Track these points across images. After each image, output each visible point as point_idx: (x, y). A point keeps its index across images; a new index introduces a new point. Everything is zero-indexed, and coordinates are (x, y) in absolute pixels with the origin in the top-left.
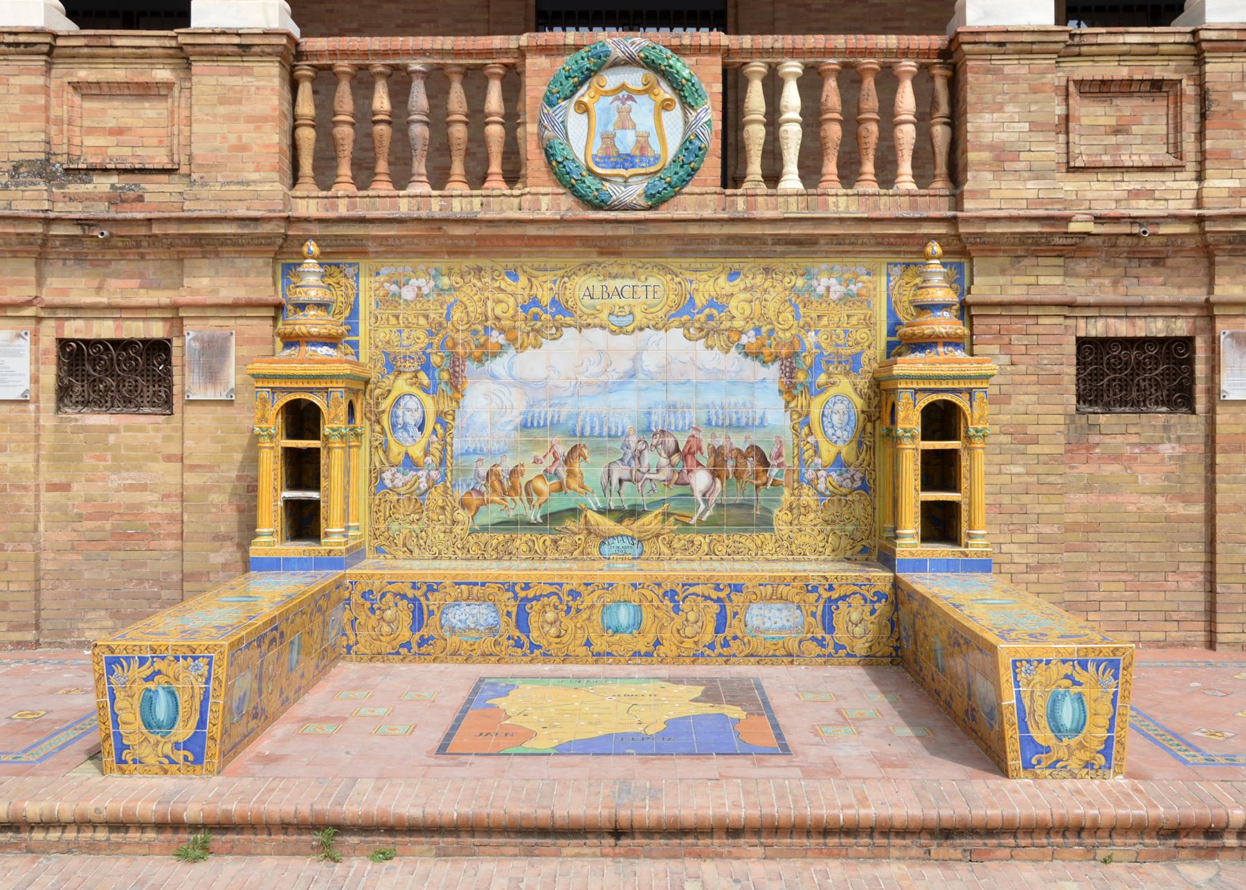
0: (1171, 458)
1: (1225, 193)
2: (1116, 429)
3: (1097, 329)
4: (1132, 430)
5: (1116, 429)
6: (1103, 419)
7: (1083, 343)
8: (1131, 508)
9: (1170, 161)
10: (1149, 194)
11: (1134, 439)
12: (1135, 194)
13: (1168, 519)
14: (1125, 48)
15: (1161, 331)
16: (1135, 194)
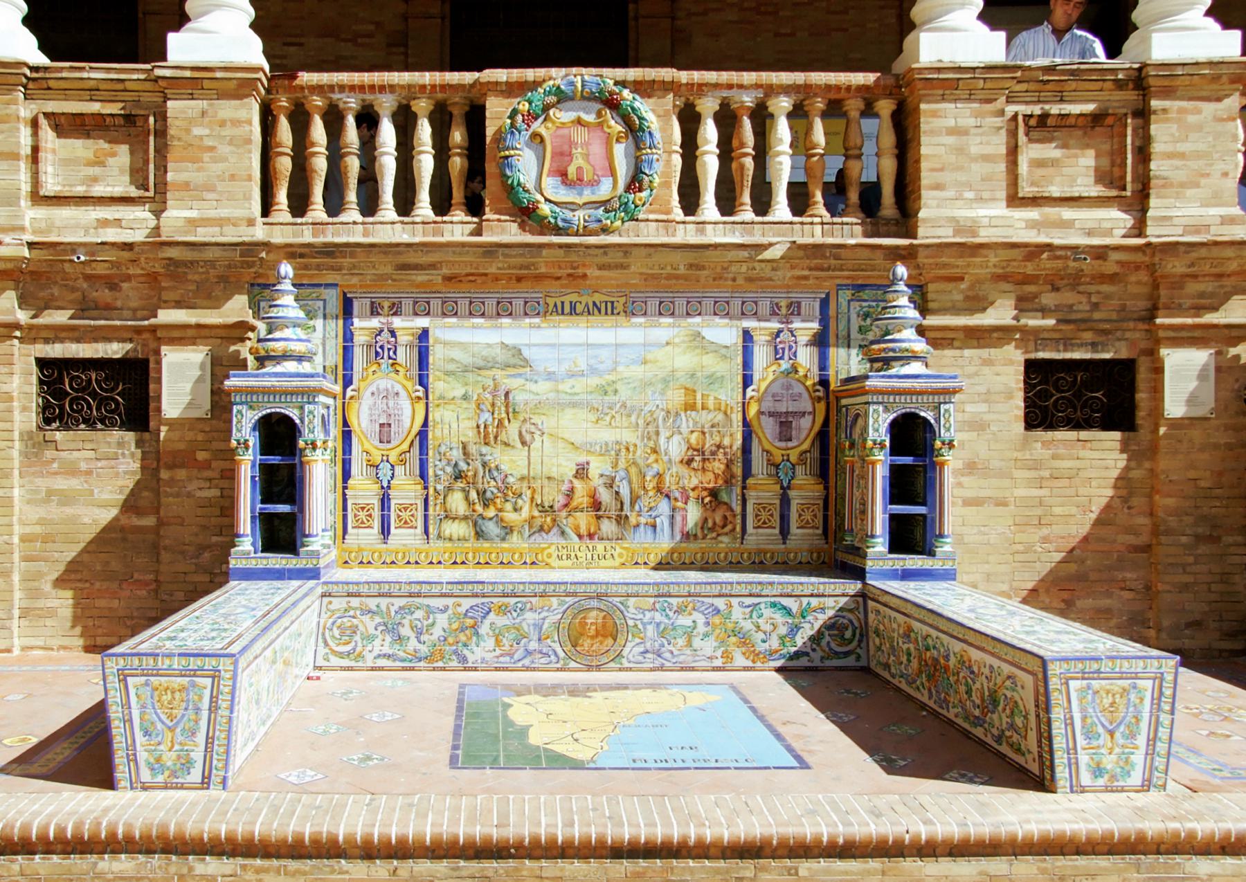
0: (126, 473)
1: (181, 223)
2: (72, 446)
3: (57, 351)
4: (90, 446)
5: (72, 446)
6: (58, 435)
7: (42, 363)
8: (86, 520)
9: (134, 192)
10: (118, 222)
11: (91, 454)
12: (104, 223)
13: (122, 529)
14: (92, 84)
15: (116, 353)
16: (104, 223)
